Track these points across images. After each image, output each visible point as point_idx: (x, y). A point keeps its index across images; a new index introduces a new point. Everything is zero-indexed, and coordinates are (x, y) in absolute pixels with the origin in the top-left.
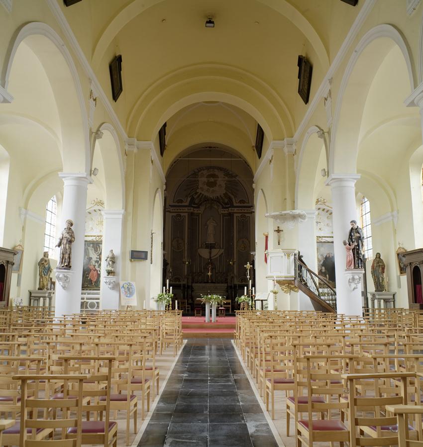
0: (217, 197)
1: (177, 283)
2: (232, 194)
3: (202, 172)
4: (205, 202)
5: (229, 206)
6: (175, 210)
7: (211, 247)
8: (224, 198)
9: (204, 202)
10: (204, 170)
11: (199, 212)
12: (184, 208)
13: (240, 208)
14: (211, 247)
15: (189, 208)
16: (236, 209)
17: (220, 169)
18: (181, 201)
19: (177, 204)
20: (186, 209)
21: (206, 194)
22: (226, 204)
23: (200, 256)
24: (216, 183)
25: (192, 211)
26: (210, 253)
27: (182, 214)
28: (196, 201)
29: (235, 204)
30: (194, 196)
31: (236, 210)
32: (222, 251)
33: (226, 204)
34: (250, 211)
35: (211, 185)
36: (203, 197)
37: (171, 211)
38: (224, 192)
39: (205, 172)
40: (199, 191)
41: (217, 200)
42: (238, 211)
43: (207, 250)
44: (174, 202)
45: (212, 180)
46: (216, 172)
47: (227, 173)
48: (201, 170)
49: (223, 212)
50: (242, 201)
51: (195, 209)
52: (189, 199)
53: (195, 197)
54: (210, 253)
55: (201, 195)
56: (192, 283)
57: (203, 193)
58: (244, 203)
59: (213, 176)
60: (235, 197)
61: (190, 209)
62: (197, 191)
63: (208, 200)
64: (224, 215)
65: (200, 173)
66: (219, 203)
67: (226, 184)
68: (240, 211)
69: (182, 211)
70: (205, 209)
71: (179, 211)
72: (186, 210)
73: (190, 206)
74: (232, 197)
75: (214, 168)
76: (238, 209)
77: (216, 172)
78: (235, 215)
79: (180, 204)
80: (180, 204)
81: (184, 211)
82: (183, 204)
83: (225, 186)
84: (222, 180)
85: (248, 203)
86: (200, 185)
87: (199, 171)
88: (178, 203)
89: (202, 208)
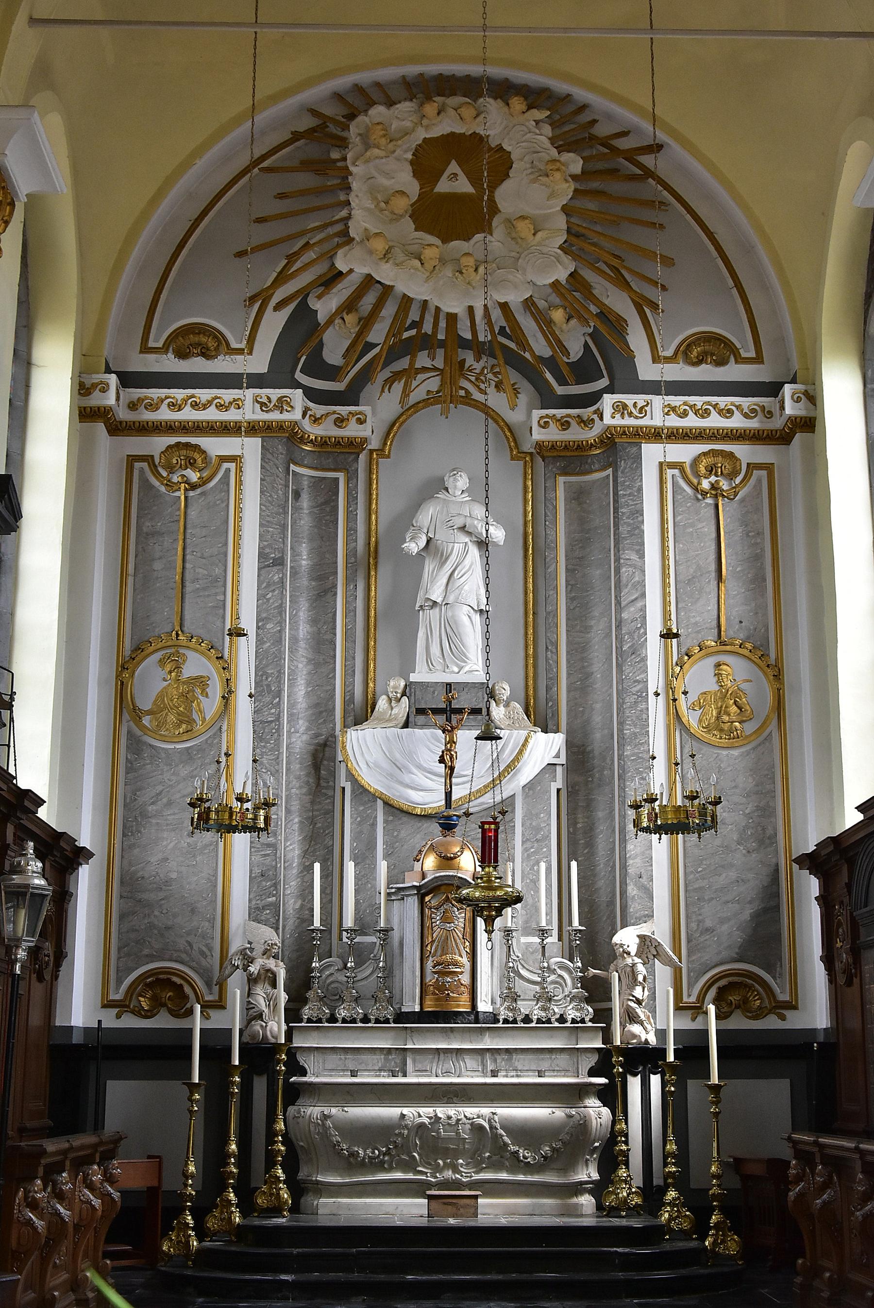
0: (504, 307)
1: (163, 1021)
2: (625, 285)
3: (378, 112)
4: (403, 363)
5: (604, 382)
6: (154, 406)
7: (447, 710)
8: (558, 315)
9: (394, 353)
10: (390, 103)
11: (352, 430)
12: (227, 395)
13: (698, 401)
14: (447, 710)
15: (275, 394)
16: (658, 401)
17: (535, 97)
18: (196, 340)
19: (170, 364)
20: (248, 406)
21: (409, 282)
22: (584, 370)
23: (362, 792)
24: (494, 210)
25: (297, 415)
26: (447, 760)
27: (216, 446)
28: (334, 349)
29: (647, 370)
30: (314, 303)
31: (657, 412)
32: (546, 748)
33: (584, 370)
34: (777, 423)
35: (450, 219)
36: (389, 311)
37: (123, 414)
38: (562, 274)
39: (416, 124)
40: (353, 263)
41: (504, 350)
42: (673, 421)
43: (428, 740)
44: (145, 349)
45: (455, 182)
46: (495, 122)
47: (571, 124)
48: (372, 103)
49: (553, 434)
50: (711, 348)
51: (319, 410)
52: (274, 323)
53: (324, 307)
54: (447, 760)
55: (368, 301)
56: (293, 1014)
57: (385, 274)
58: (721, 362)
59: (466, 149)
60: (642, 304)
61: (282, 404)
62: (341, 265)
63: (426, 342)
64: (567, 458)
65: (354, 129)
66: (529, 371)
67: (565, 209)
68: (692, 421)
69: (212, 415)
70: (410, 410)
71: (188, 414)
72: (250, 413)
73: (278, 375)
74: (620, 303)
75: (470, 87)
76: (676, 401)
77: (495, 122)
78: (652, 454)
79: (197, 365)
80: (197, 365)
81: (232, 415)
82: (222, 365)
83: (561, 222)
84: (538, 194)
85: (758, 359)
86: (361, 221)
87: (352, 116)
88: (182, 355)
89: (377, 411)
